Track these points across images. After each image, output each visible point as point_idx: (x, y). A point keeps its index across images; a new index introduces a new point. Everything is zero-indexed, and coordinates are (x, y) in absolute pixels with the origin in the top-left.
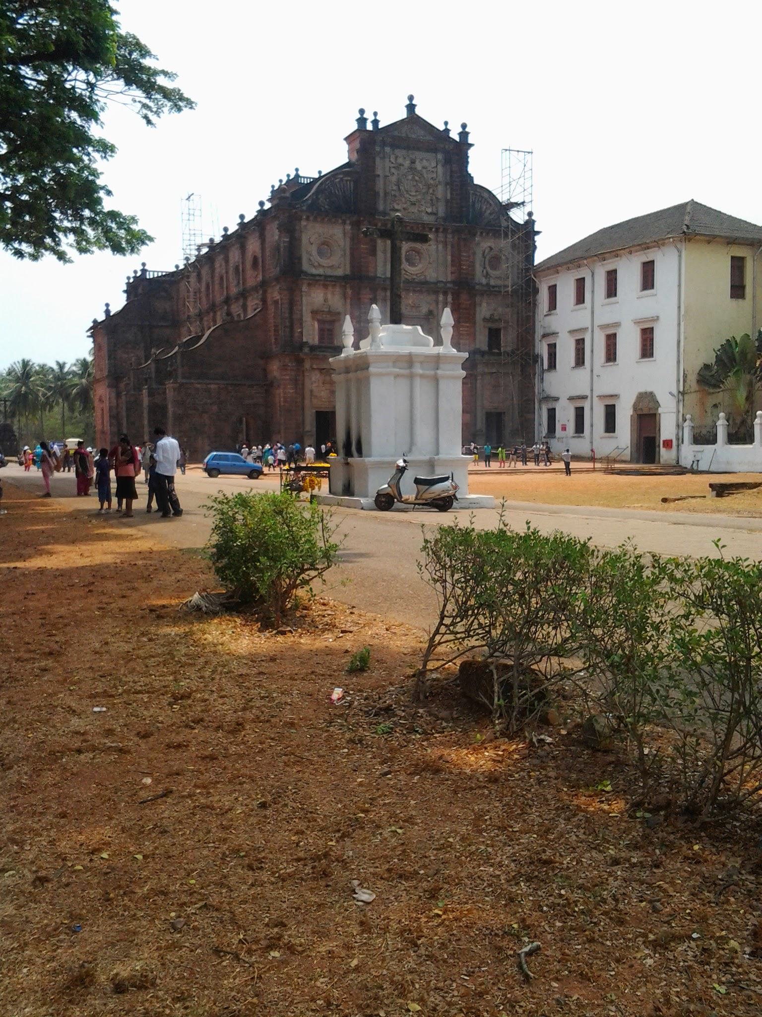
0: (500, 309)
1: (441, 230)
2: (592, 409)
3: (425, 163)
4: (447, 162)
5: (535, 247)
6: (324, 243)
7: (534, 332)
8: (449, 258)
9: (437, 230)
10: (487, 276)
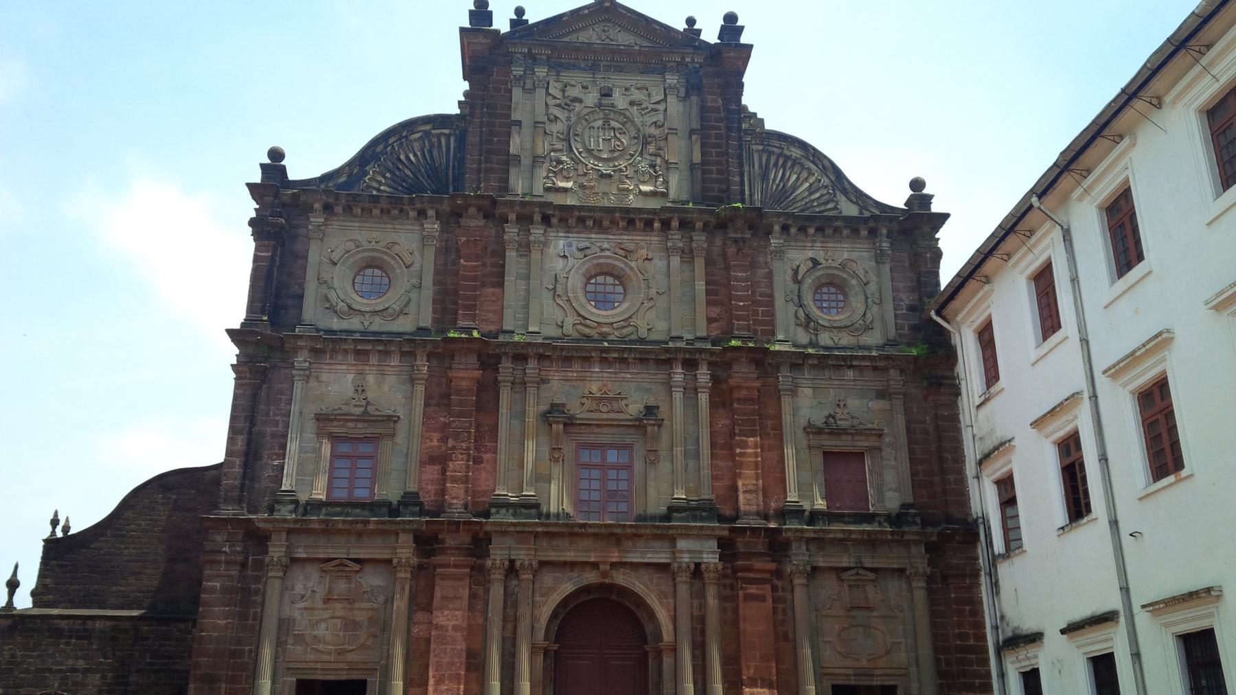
0: (854, 404)
1: (675, 223)
2: (1136, 656)
3: (637, 95)
4: (693, 88)
5: (938, 255)
6: (371, 264)
7: (959, 459)
8: (701, 286)
9: (666, 225)
10: (808, 322)
